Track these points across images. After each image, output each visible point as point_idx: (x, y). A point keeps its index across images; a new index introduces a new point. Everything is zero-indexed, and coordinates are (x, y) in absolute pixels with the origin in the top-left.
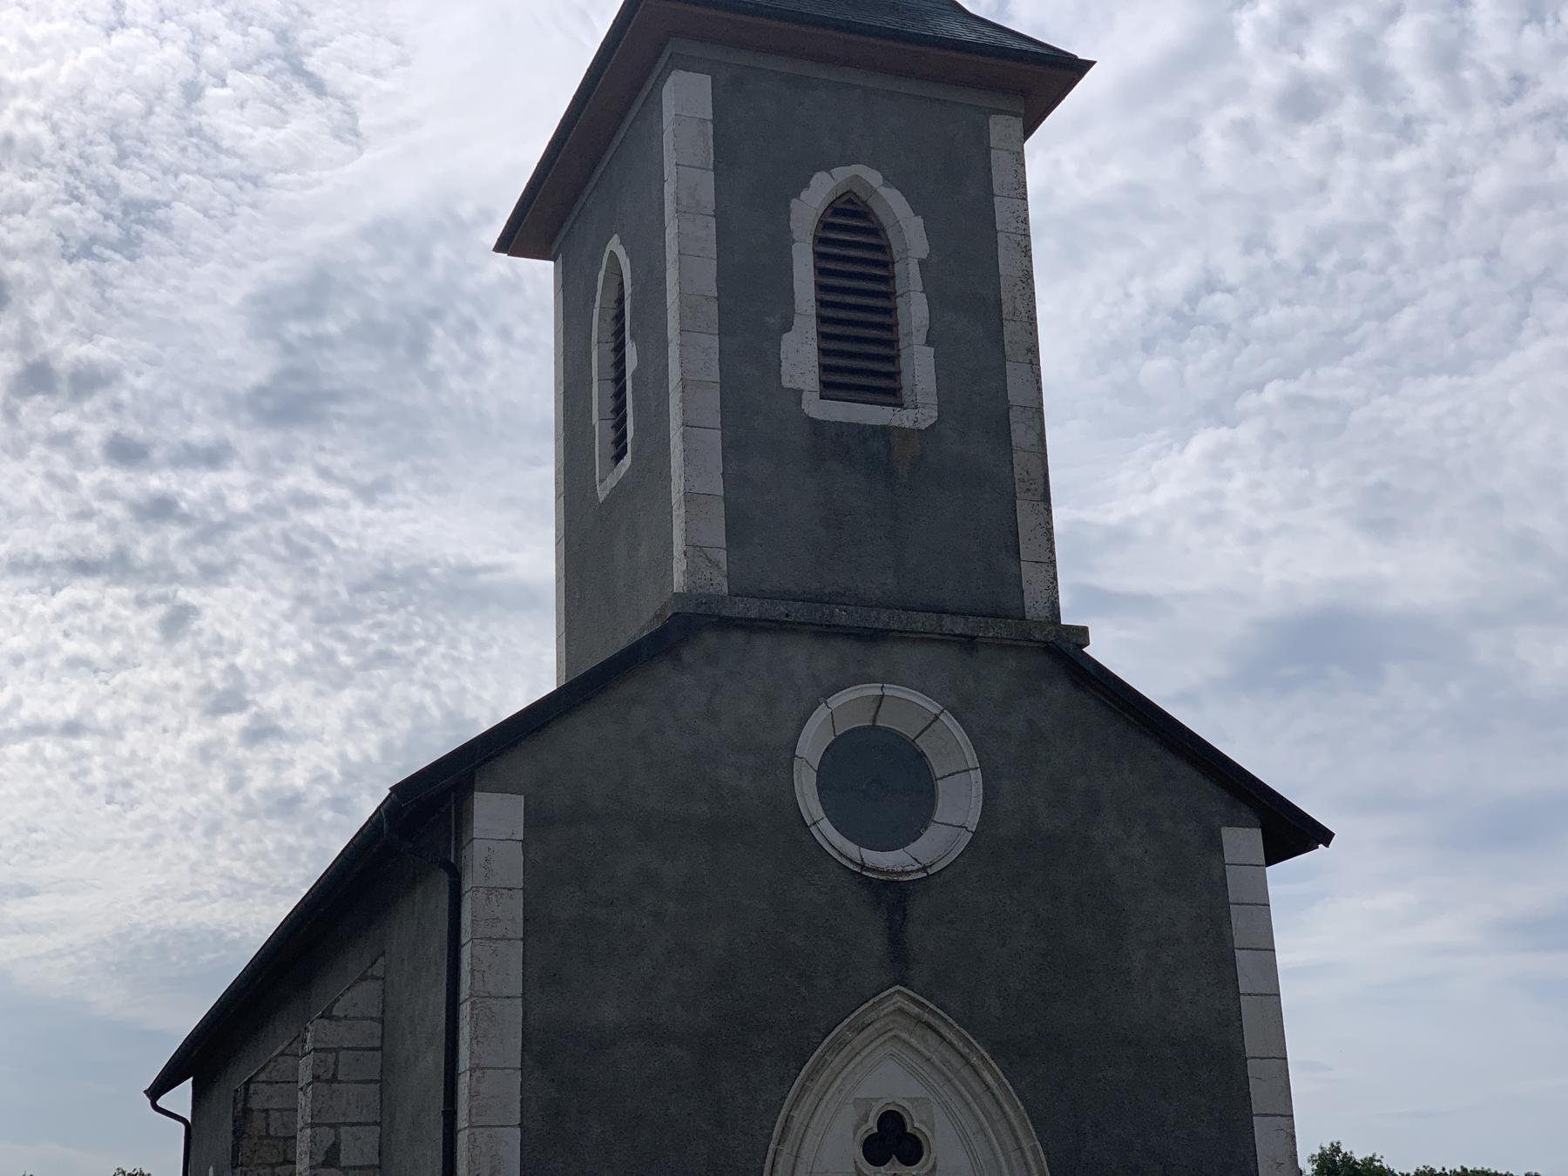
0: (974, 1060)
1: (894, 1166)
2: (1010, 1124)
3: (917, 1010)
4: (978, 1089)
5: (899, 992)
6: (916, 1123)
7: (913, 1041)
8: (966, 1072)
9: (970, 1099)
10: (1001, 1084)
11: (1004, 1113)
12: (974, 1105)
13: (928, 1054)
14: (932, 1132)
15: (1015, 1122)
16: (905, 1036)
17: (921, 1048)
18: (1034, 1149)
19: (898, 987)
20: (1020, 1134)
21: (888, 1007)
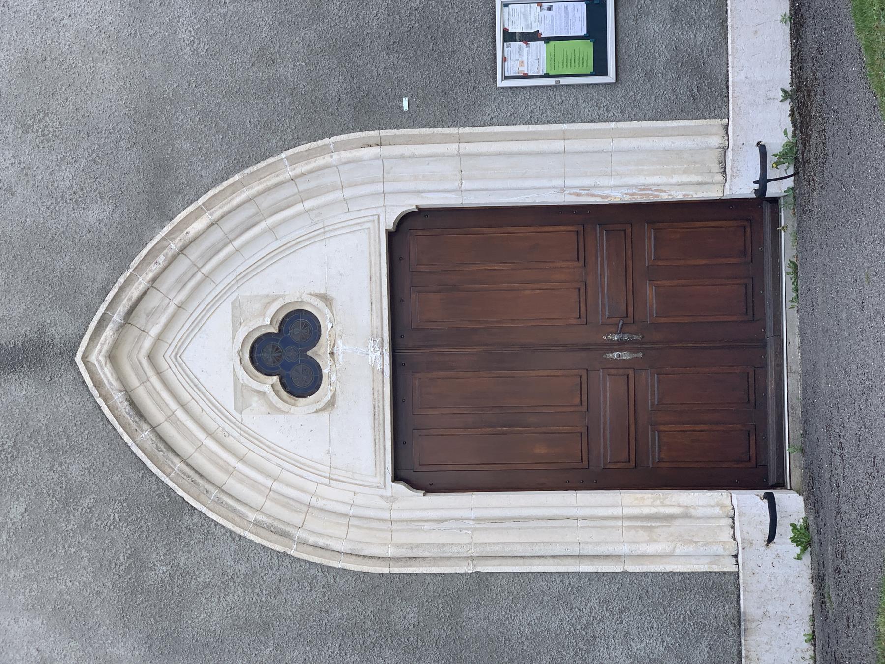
0: (174, 246)
1: (320, 353)
2: (260, 194)
3: (108, 333)
4: (216, 235)
5: (84, 358)
6: (266, 322)
7: (154, 331)
8: (194, 253)
9: (229, 249)
10: (208, 206)
11: (249, 200)
12: (237, 243)
13: (171, 309)
14: (275, 299)
15: (257, 187)
16: (147, 344)
17: (163, 320)
18: (294, 160)
19: (78, 359)
20: (274, 180)
21: (106, 374)
